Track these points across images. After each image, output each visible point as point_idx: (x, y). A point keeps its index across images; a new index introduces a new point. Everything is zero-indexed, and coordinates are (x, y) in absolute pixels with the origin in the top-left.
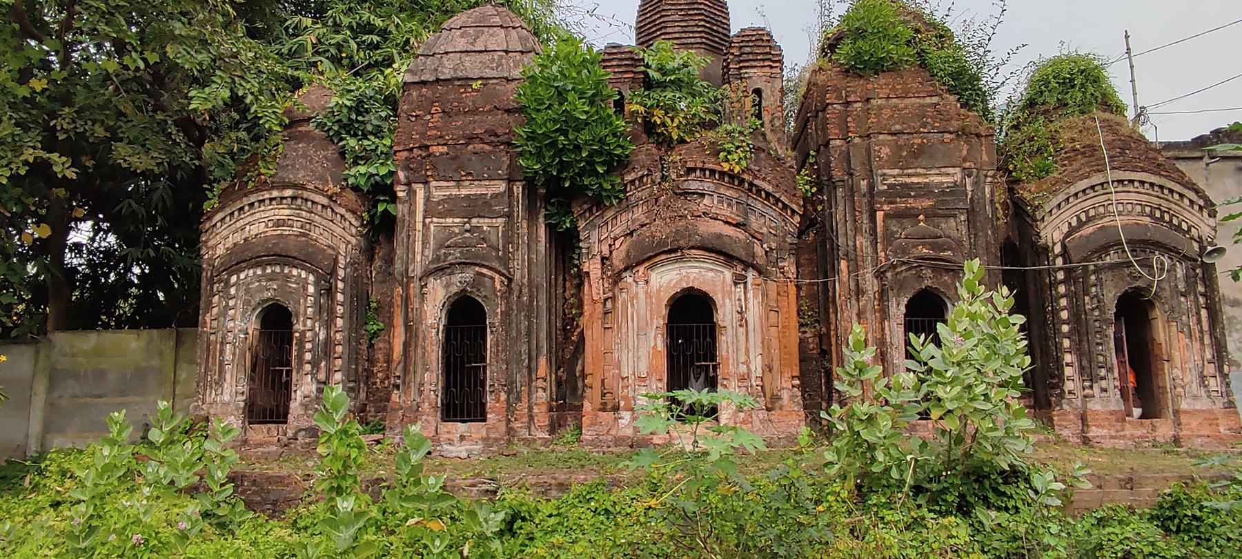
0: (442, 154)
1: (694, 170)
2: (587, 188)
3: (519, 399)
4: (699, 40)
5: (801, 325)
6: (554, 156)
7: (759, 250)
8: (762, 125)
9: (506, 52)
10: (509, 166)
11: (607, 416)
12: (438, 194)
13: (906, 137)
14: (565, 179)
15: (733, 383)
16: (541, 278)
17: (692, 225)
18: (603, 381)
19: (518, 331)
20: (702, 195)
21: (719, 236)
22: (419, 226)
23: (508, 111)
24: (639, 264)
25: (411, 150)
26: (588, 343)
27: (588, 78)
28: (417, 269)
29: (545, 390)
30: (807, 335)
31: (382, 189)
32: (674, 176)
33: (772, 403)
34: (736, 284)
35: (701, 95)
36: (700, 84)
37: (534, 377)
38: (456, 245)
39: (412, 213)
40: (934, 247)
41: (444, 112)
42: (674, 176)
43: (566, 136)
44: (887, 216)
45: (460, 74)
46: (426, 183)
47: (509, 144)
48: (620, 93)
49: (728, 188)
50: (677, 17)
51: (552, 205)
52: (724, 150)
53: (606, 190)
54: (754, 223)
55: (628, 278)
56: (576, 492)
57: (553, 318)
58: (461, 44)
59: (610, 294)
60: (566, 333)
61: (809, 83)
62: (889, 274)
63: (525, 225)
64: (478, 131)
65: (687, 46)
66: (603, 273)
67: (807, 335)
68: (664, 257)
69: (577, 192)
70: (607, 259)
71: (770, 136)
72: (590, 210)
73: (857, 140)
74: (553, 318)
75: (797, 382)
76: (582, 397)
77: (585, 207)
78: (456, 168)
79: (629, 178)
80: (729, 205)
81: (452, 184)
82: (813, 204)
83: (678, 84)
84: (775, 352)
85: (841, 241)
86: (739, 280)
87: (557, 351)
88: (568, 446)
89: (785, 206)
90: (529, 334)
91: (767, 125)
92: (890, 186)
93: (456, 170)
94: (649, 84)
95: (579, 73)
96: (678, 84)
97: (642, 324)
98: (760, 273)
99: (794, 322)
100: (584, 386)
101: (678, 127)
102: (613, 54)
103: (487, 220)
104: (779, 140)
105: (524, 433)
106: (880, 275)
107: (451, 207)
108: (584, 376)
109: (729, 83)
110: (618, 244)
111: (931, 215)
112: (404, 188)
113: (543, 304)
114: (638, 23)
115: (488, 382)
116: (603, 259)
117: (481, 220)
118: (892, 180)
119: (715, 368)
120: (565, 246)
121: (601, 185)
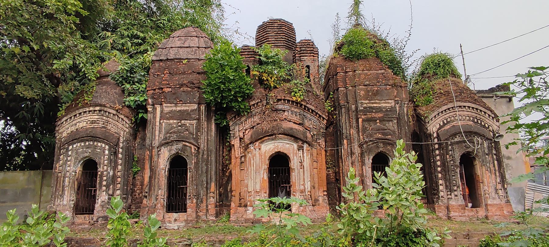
0: (169, 92)
1: (281, 100)
2: (233, 107)
3: (202, 202)
4: (283, 44)
5: (327, 168)
6: (219, 93)
7: (309, 135)
8: (310, 81)
9: (198, 47)
10: (199, 97)
11: (243, 209)
12: (166, 110)
13: (371, 87)
14: (224, 104)
15: (298, 194)
16: (213, 147)
17: (280, 124)
18: (240, 193)
19: (202, 171)
20: (284, 111)
21: (292, 129)
22: (158, 124)
23: (198, 73)
24: (256, 141)
25: (155, 90)
26: (233, 176)
27: (234, 60)
28: (156, 143)
29: (214, 198)
30: (330, 172)
31: (141, 107)
32: (272, 103)
33: (315, 202)
34: (299, 150)
35: (284, 68)
36: (283, 63)
37: (209, 192)
38: (174, 132)
39: (155, 118)
40: (383, 134)
41: (170, 73)
42: (272, 103)
43: (224, 84)
44: (363, 120)
45: (178, 57)
46: (161, 104)
47: (199, 88)
48: (248, 66)
49: (296, 108)
50: (273, 34)
51: (218, 115)
52: (293, 91)
53: (242, 108)
54: (307, 123)
55: (252, 147)
56: (227, 244)
57: (218, 165)
58: (178, 44)
59: (243, 154)
60: (224, 172)
61: (330, 63)
62: (364, 146)
63: (206, 124)
64: (185, 82)
65: (277, 46)
66: (240, 145)
67: (330, 172)
68: (267, 138)
69: (229, 109)
70: (242, 139)
71: (313, 86)
72: (235, 117)
73: (350, 88)
74: (218, 165)
75: (326, 193)
76: (231, 201)
77: (233, 116)
78: (175, 98)
79: (252, 103)
80: (296, 115)
81: (173, 105)
82: (332, 116)
83: (274, 63)
84: (316, 180)
85: (344, 131)
86: (300, 148)
87: (219, 180)
88: (224, 223)
89: (320, 116)
90: (207, 172)
91: (312, 81)
92: (365, 108)
93: (175, 99)
94: (261, 63)
95: (230, 58)
96: (274, 63)
97: (258, 167)
98: (309, 145)
99: (324, 166)
100: (232, 196)
101: (273, 81)
102: (245, 50)
103: (188, 121)
104: (317, 88)
105: (204, 218)
106: (361, 146)
107: (172, 115)
108: (231, 191)
109: (296, 63)
110: (247, 132)
111: (382, 120)
112: (151, 106)
113: (213, 159)
114: (256, 36)
115: (188, 194)
116: (240, 139)
117: (186, 121)
118: (365, 105)
119: (290, 187)
120: (223, 133)
121: (240, 106)
